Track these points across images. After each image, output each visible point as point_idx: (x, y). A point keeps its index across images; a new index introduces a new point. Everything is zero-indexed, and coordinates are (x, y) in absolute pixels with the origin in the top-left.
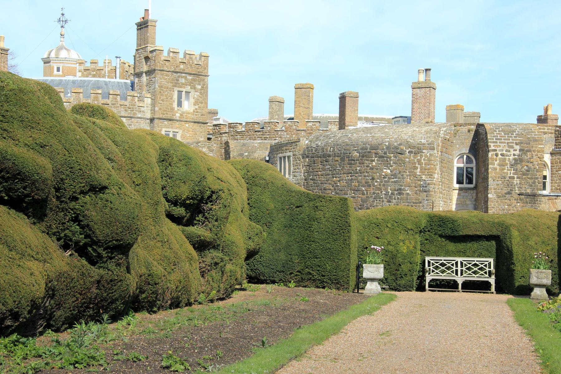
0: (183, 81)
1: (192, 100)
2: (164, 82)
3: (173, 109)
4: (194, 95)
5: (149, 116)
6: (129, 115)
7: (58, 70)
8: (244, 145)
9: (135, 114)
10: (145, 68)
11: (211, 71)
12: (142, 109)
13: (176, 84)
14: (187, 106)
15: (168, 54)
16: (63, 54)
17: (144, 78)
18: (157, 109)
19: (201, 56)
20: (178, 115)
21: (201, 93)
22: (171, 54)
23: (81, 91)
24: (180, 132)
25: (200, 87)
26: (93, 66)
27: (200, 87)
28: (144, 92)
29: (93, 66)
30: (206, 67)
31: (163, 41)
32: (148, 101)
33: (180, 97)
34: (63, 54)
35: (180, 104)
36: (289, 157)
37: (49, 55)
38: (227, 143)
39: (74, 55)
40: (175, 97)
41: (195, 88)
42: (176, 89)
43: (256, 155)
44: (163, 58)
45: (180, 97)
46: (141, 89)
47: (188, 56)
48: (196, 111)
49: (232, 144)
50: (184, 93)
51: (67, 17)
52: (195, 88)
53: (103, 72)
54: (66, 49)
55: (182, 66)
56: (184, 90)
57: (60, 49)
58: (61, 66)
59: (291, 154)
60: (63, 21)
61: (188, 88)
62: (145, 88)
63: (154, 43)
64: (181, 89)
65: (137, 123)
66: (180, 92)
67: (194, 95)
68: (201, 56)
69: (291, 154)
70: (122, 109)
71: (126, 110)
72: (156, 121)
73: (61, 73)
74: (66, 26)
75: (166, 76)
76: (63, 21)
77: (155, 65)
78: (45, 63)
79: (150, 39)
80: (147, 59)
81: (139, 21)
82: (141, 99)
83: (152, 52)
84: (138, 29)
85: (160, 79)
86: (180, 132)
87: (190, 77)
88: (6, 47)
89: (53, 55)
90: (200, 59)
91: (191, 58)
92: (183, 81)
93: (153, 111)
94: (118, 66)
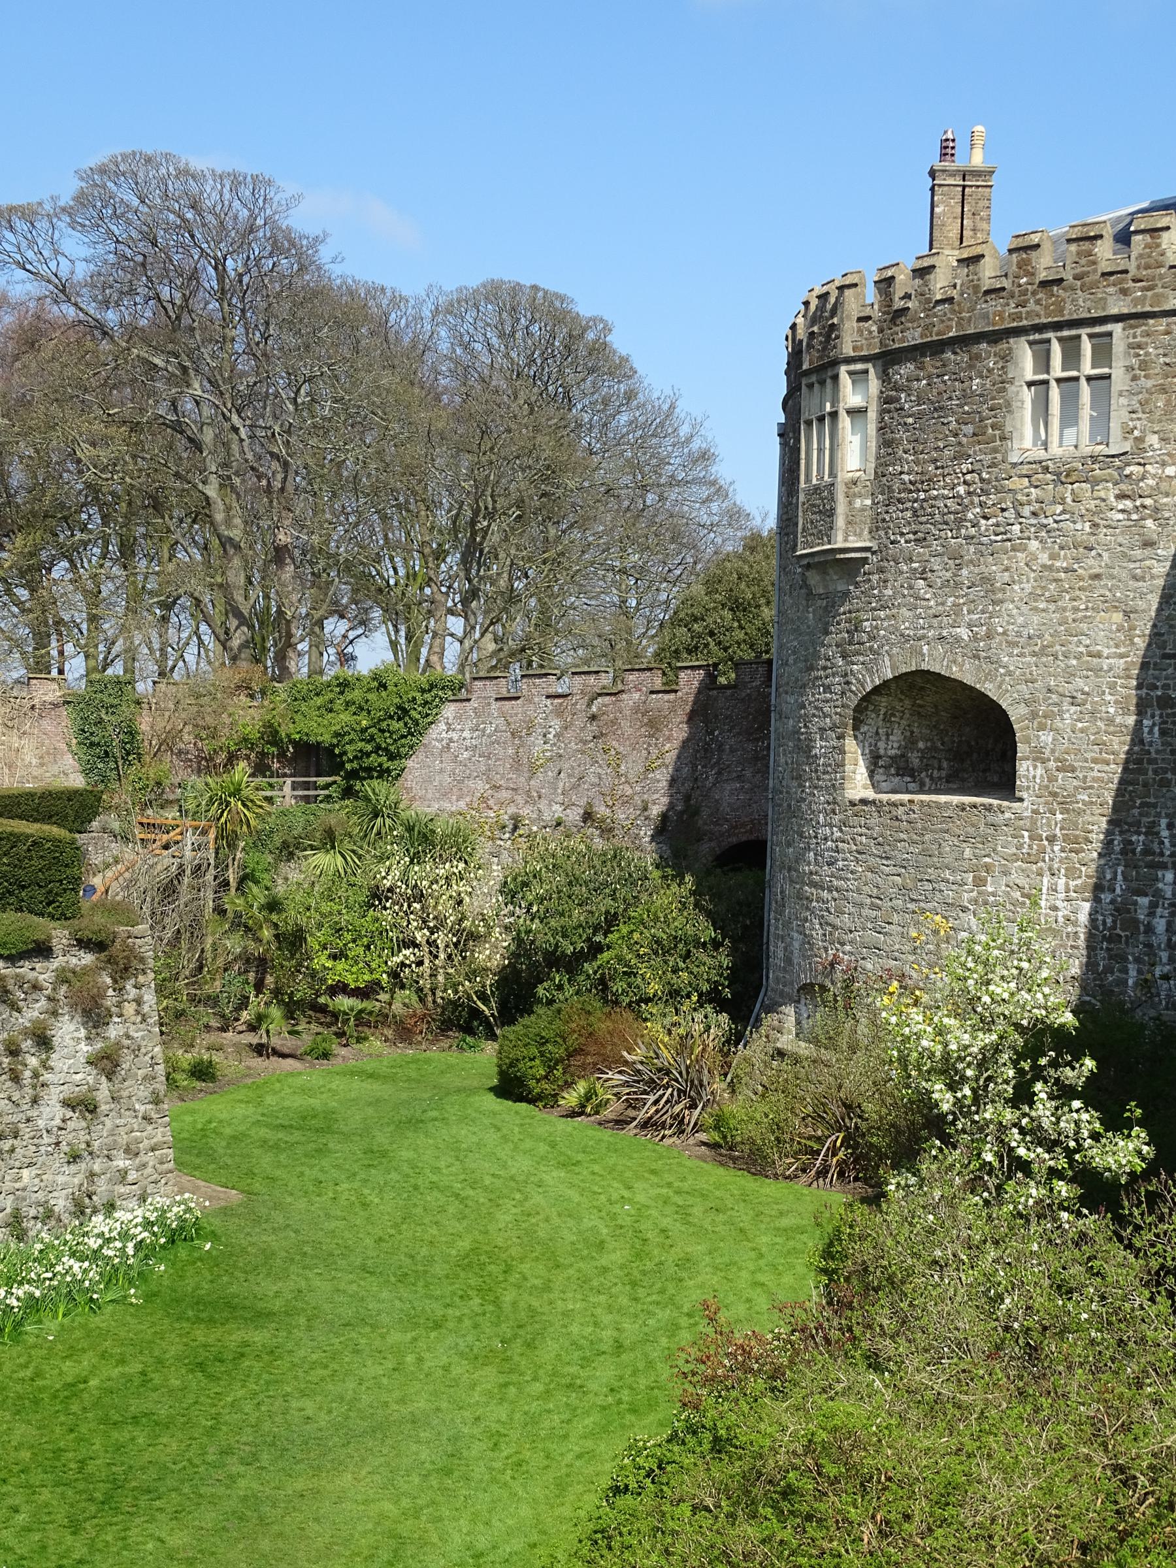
6: (1139, 309)
65: (1167, 333)
70: (1111, 290)
71: (1124, 292)
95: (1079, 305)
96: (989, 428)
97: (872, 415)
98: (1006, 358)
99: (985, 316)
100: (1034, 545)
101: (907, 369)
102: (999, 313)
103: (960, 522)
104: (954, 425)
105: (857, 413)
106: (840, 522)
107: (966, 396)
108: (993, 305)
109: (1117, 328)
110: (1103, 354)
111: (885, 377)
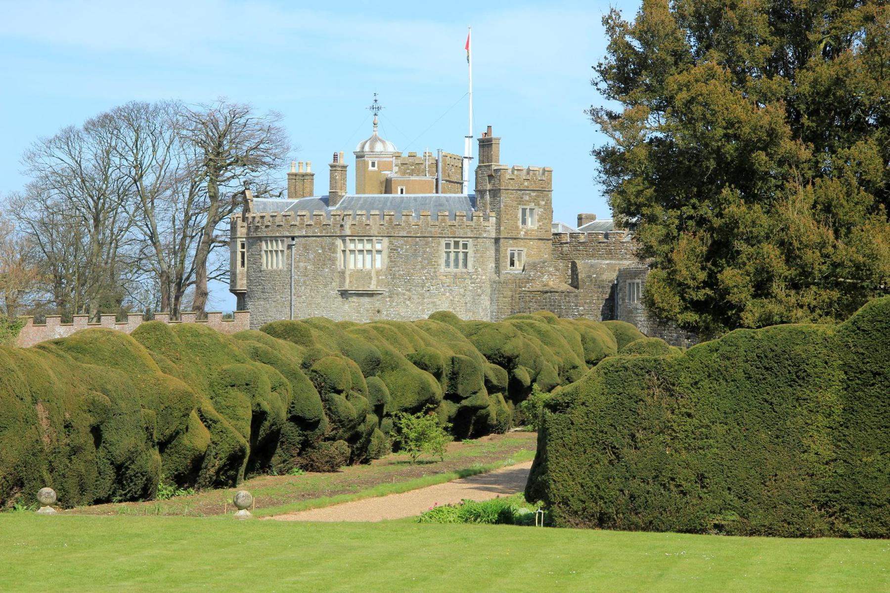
0: (527, 198)
1: (536, 217)
2: (509, 201)
3: (517, 227)
4: (538, 211)
5: (493, 235)
7: (373, 165)
8: (592, 266)
9: (480, 234)
10: (489, 187)
11: (554, 186)
12: (488, 229)
13: (520, 201)
14: (532, 224)
15: (513, 172)
16: (379, 147)
17: (488, 196)
18: (502, 228)
19: (544, 170)
20: (522, 233)
21: (545, 209)
22: (516, 172)
23: (429, 213)
24: (525, 250)
25: (543, 203)
26: (411, 160)
27: (543, 203)
28: (488, 211)
29: (411, 160)
30: (549, 182)
31: (507, 158)
32: (493, 220)
33: (524, 214)
34: (379, 147)
35: (524, 222)
36: (638, 284)
37: (363, 147)
38: (574, 265)
39: (391, 148)
40: (520, 215)
41: (539, 205)
42: (521, 207)
43: (604, 277)
44: (508, 177)
45: (524, 214)
46: (484, 205)
47: (531, 173)
48: (540, 228)
49: (580, 264)
50: (528, 211)
51: (379, 104)
52: (539, 205)
53: (423, 167)
54: (380, 140)
55: (526, 184)
56: (528, 207)
57: (374, 140)
58: (376, 161)
59: (640, 281)
60: (376, 109)
61: (532, 205)
62: (488, 206)
63: (497, 161)
64: (525, 207)
66: (524, 210)
67: (538, 211)
68: (544, 170)
69: (640, 281)
72: (502, 241)
73: (376, 168)
74: (379, 113)
75: (512, 194)
76: (376, 109)
77: (500, 184)
78: (357, 157)
79: (494, 158)
80: (491, 177)
81: (481, 137)
82: (486, 219)
83: (496, 171)
84: (480, 146)
85: (505, 199)
86: (525, 250)
87: (533, 194)
88: (346, 164)
89: (367, 148)
90: (543, 174)
91: (534, 174)
92: (527, 198)
93: (498, 230)
94: (440, 160)
95: (460, 232)
96: (431, 262)
97: (385, 253)
98: (439, 244)
99: (431, 232)
100: (448, 294)
101: (401, 241)
102: (436, 231)
103: (423, 287)
104: (420, 259)
105: (379, 252)
106: (374, 282)
107: (424, 252)
108: (433, 230)
109: (470, 240)
110: (465, 246)
111: (391, 243)
